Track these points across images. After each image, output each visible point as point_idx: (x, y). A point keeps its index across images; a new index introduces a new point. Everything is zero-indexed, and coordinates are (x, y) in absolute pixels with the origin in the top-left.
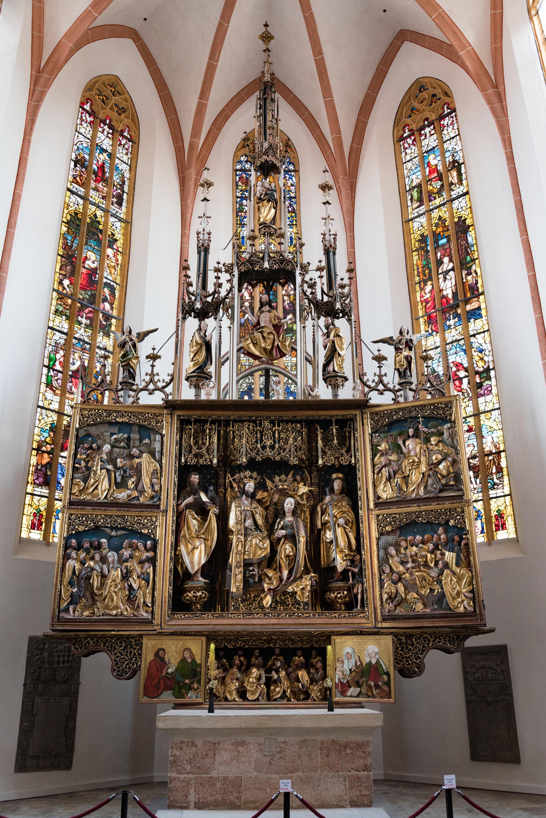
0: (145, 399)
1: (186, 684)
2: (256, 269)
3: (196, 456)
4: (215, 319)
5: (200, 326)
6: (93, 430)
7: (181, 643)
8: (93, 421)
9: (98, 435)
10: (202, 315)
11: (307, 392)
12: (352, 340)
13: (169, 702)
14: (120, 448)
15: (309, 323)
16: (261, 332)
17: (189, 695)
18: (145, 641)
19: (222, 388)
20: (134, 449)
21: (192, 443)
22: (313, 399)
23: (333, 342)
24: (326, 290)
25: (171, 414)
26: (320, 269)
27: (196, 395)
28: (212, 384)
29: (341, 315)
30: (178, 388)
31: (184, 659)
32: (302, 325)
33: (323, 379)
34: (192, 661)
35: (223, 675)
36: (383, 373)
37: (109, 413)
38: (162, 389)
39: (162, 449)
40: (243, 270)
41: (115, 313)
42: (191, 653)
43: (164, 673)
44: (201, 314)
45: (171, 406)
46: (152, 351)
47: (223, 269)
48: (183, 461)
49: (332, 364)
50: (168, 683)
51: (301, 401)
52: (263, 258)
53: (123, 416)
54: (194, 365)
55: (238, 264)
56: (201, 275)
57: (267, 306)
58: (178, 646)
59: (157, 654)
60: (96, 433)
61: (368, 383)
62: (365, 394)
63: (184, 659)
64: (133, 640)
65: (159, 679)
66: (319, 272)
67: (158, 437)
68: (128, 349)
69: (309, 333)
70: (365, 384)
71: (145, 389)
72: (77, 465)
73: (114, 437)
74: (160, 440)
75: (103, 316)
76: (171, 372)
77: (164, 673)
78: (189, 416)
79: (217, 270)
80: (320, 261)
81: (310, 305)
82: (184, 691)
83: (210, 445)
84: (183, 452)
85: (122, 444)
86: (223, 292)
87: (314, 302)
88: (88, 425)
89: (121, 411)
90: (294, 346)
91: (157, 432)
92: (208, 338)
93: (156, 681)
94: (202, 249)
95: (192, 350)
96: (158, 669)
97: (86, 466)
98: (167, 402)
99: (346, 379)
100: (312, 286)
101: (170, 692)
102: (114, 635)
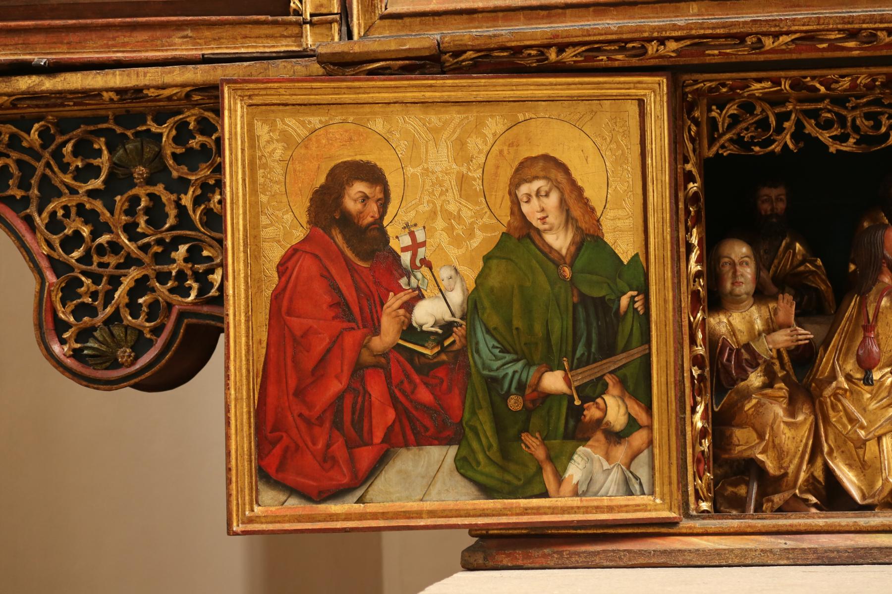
1: (548, 396)
7: (494, 124)
13: (439, 525)
17: (575, 472)
18: (234, 118)
31: (522, 235)
34: (579, 246)
35: (805, 334)
42: (573, 196)
43: (388, 333)
50: (424, 395)
58: (475, 144)
59: (326, 205)
63: (522, 235)
64: (166, 131)
65: (358, 369)
77: (388, 333)
82: (534, 445)
93: (335, 387)
96: (341, 306)
101: (440, 456)
102: (33, 96)
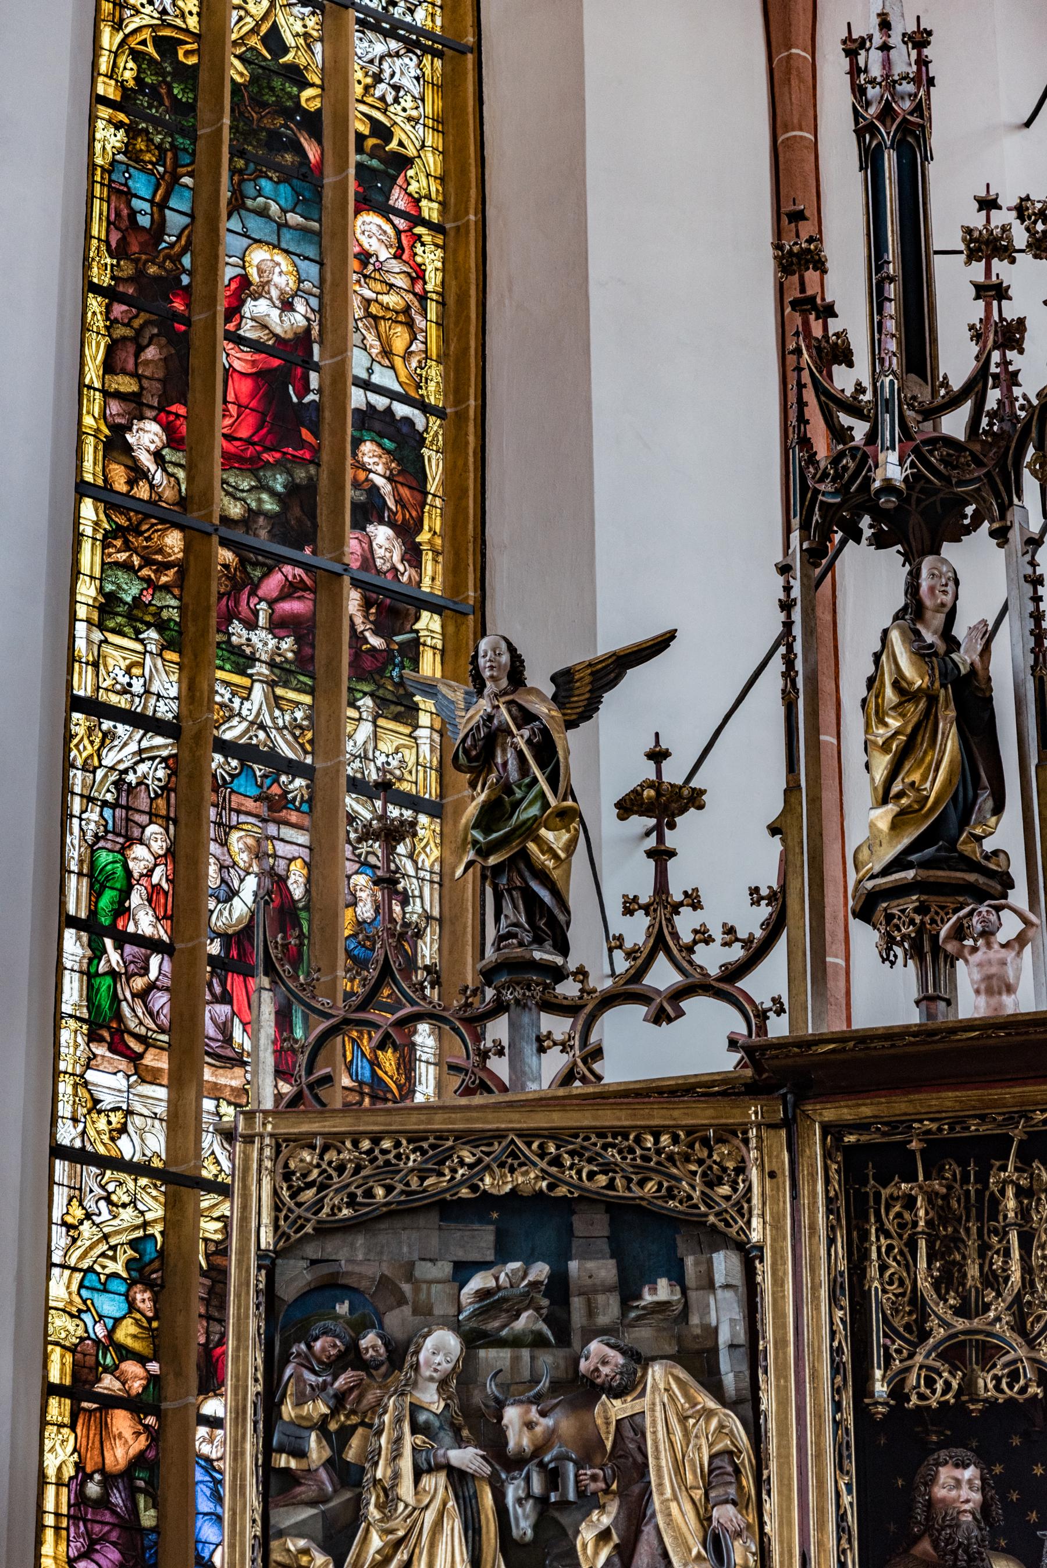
0: (634, 1050)
3: (954, 1353)
4: (1001, 535)
6: (357, 1258)
8: (352, 1202)
9: (384, 1282)
14: (515, 1342)
20: (594, 1346)
21: (924, 1284)
25: (788, 1123)
27: (926, 1000)
28: (1010, 926)
30: (817, 971)
37: (436, 1146)
38: (725, 985)
39: (754, 1333)
41: (431, 579)
44: (915, 520)
45: (783, 1075)
46: (649, 771)
48: (880, 1389)
53: (513, 1161)
54: (897, 824)
60: (372, 1270)
67: (725, 1265)
68: (514, 775)
71: (628, 991)
72: (283, 1461)
73: (478, 1282)
74: (738, 1279)
75: (367, 604)
76: (769, 879)
78: (894, 1126)
83: (1028, 1283)
84: (877, 1337)
85: (524, 1321)
88: (324, 1231)
89: (499, 1135)
91: (717, 1238)
95: (881, 733)
97: (336, 1464)
98: (755, 1051)
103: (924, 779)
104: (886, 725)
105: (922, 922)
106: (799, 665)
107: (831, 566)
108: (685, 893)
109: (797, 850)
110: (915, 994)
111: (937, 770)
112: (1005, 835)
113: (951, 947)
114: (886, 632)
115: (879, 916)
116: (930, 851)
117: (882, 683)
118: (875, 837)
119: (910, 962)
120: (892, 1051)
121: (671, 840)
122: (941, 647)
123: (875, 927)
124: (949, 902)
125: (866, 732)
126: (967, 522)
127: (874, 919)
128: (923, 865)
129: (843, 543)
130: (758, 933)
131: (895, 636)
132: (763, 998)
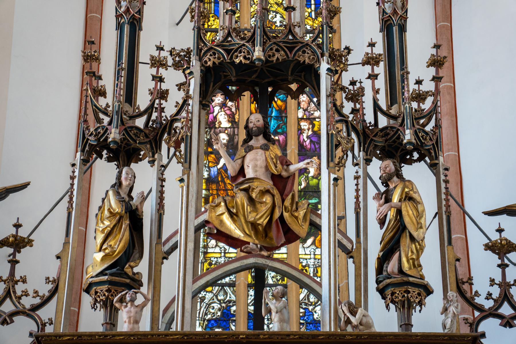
2: (237, 61)
5: (119, 177)
10: (124, 154)
11: (342, 317)
12: (440, 207)
15: (350, 171)
16: (246, 190)
19: (163, 306)
22: (356, 331)
23: (399, 212)
24: (383, 104)
26: (371, 60)
28: (140, 300)
29: (416, 155)
32: (333, 176)
33: (378, 290)
36: (510, 279)
40: (210, 63)
46: (13, 231)
47: (170, 62)
49: (397, 255)
51: (329, 335)
52: (252, 40)
54: (103, 259)
55: (199, 50)
56: (123, 73)
57: (261, 137)
61: (478, 300)
62: (471, 325)
66: (368, 69)
69: (348, 192)
70: (470, 302)
76: (53, 275)
79: (157, 63)
80: (372, 45)
81: (349, 135)
86: (170, 109)
87: (359, 127)
90: (317, 220)
92: (135, 202)
94: (125, 19)
99: (429, 291)
100: (356, 97)
103: (115, 244)
104: (103, 224)
105: (108, 296)
106: (74, 199)
107: (91, 166)
108: (21, 277)
109: (66, 265)
110: (102, 322)
111: (120, 241)
112: (142, 268)
113: (117, 305)
114: (107, 191)
115: (93, 291)
116: (114, 270)
117: (104, 209)
118: (95, 263)
119: (102, 310)
120: (91, 341)
121: (18, 257)
122: (127, 199)
123: (90, 295)
124: (119, 289)
125: (96, 225)
126: (141, 157)
127: (91, 293)
128: (112, 275)
129: (96, 159)
130: (47, 294)
131: (111, 193)
132: (45, 318)
